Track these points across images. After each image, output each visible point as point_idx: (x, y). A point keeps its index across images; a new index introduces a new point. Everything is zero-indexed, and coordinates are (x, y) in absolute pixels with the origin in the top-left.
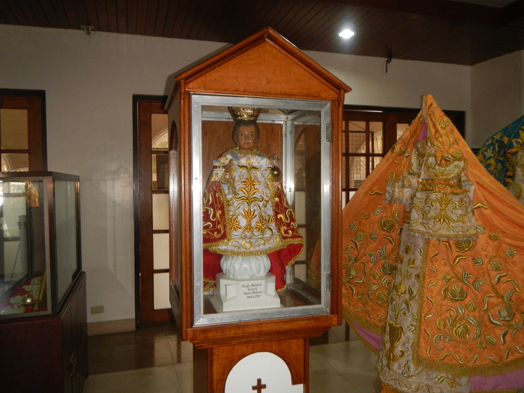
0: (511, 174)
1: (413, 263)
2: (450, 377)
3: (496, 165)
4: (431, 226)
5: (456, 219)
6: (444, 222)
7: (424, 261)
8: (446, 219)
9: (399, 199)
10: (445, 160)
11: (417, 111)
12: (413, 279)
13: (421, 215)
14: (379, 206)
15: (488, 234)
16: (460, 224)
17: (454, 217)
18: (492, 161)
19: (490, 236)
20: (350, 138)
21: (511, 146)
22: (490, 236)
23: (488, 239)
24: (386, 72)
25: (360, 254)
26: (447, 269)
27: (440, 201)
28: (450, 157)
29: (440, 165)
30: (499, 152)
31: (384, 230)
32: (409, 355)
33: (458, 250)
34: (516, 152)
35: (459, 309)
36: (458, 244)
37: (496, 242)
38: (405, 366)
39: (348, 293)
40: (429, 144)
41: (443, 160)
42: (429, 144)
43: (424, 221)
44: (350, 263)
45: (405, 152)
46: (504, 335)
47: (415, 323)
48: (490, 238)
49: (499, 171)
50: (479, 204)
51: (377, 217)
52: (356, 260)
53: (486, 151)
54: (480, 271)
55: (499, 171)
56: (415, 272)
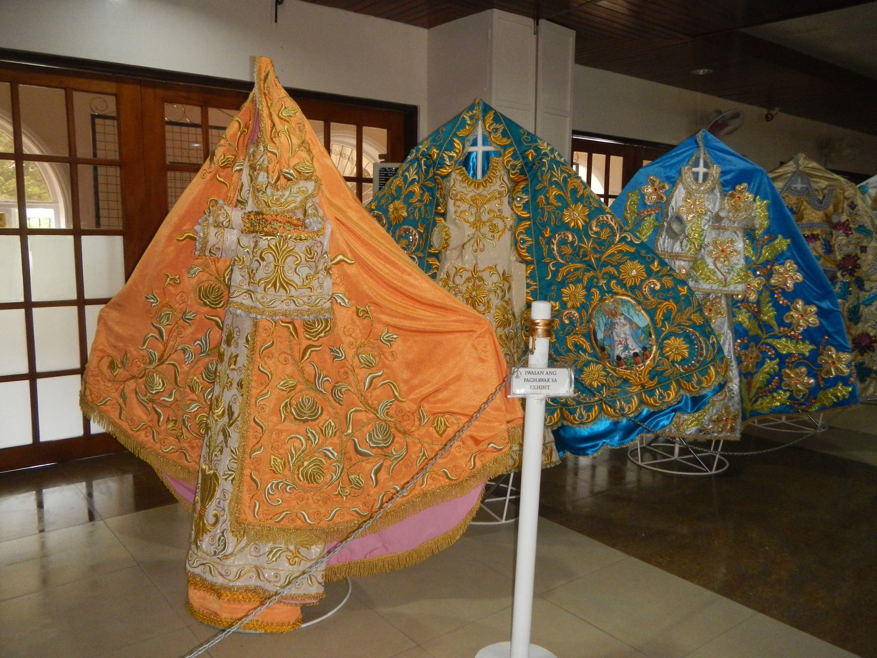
0: (443, 211)
1: (235, 362)
2: (292, 548)
3: (422, 195)
4: (259, 296)
5: (299, 284)
6: (281, 290)
7: (251, 359)
8: (285, 284)
9: (218, 249)
10: (285, 177)
11: (250, 86)
12: (234, 390)
13: (247, 277)
14: (196, 262)
15: (354, 308)
16: (307, 292)
17: (295, 278)
18: (416, 188)
19: (358, 310)
21: (442, 165)
22: (358, 310)
23: (355, 316)
24: (276, 21)
25: (168, 349)
26: (289, 369)
27: (277, 251)
28: (292, 172)
29: (275, 186)
30: (427, 172)
31: (205, 304)
32: (225, 524)
33: (308, 336)
34: (449, 174)
35: (310, 435)
36: (308, 326)
37: (366, 321)
38: (219, 539)
39: (151, 421)
40: (262, 148)
41: (282, 177)
42: (262, 148)
43: (251, 288)
44: (152, 367)
45: (234, 161)
46: (377, 472)
47: (235, 466)
48: (358, 315)
49: (426, 205)
50: (340, 257)
51: (194, 281)
52: (161, 361)
53: (408, 170)
54: (342, 370)
55: (426, 205)
56: (236, 377)
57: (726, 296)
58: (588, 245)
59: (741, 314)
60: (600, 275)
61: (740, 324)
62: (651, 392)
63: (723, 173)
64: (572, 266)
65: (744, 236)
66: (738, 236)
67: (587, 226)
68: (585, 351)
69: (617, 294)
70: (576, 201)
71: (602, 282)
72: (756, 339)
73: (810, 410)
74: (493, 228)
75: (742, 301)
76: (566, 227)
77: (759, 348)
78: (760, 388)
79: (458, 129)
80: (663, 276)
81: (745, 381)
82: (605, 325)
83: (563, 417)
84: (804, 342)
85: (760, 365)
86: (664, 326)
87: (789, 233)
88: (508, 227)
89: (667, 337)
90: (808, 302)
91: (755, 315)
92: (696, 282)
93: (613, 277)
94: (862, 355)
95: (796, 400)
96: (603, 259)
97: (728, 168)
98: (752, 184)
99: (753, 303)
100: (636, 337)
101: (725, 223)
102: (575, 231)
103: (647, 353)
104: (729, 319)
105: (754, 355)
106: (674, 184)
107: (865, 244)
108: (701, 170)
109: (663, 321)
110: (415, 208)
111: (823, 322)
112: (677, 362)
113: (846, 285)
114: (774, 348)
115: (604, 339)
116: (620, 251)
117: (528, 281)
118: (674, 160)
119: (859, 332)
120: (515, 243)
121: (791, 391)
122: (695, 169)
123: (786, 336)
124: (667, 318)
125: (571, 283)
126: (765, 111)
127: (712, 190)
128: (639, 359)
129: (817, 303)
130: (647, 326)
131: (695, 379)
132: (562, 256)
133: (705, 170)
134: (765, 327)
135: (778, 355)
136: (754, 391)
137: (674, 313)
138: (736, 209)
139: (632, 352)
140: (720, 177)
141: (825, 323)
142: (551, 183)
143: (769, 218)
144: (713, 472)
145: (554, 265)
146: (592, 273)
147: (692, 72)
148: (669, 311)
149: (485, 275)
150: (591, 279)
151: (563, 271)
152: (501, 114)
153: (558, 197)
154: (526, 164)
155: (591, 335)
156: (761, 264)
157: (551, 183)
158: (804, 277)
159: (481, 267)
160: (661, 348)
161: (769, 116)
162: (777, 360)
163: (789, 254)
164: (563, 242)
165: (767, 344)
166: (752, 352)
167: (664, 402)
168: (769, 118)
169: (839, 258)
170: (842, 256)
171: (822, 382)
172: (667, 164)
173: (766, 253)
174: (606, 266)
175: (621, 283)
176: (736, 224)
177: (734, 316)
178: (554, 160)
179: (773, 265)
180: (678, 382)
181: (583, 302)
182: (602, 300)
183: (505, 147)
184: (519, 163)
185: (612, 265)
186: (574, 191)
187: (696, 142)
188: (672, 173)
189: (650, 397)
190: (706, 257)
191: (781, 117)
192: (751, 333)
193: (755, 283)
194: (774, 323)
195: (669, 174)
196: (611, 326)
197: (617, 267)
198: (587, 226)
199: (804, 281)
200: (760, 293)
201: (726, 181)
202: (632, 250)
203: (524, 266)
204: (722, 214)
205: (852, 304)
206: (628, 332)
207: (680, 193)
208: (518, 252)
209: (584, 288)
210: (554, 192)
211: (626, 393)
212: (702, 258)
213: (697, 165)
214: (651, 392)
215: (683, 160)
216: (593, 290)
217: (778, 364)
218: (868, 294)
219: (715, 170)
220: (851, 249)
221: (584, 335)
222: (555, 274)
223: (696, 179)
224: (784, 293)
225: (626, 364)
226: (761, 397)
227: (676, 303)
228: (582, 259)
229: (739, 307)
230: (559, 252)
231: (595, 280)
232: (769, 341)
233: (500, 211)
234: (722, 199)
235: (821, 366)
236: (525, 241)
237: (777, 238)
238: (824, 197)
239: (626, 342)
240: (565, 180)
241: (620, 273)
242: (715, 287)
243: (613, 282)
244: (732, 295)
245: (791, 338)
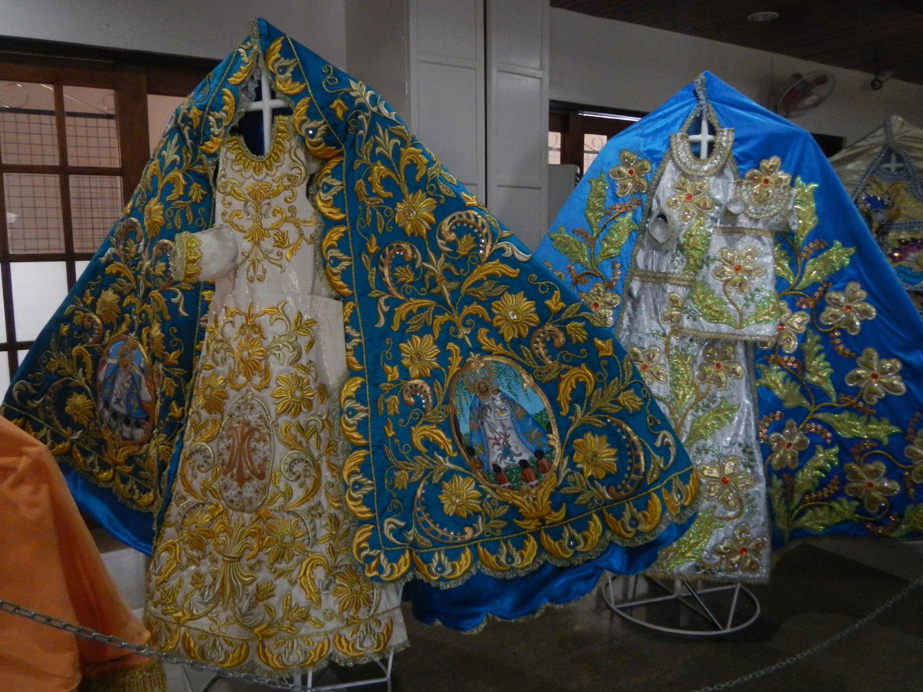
3: (187, 188)
20: (69, 130)
57: (745, 343)
58: (437, 266)
59: (771, 371)
60: (458, 319)
61: (768, 389)
62: (556, 534)
63: (738, 141)
64: (415, 304)
65: (775, 244)
66: (764, 244)
67: (434, 228)
68: (443, 453)
69: (489, 353)
70: (414, 188)
71: (464, 332)
72: (798, 414)
73: (894, 535)
74: (282, 241)
75: (773, 351)
76: (400, 233)
77: (803, 429)
78: (808, 493)
79: (229, 75)
80: (569, 320)
81: (778, 483)
82: (471, 409)
83: (413, 566)
84: (879, 420)
85: (805, 455)
86: (572, 412)
87: (852, 238)
88: (308, 236)
89: (578, 434)
90: (886, 354)
91: (796, 375)
92: (695, 320)
93: (480, 322)
95: (867, 514)
96: (463, 289)
97: (745, 132)
98: (789, 156)
99: (790, 355)
100: (524, 435)
101: (743, 222)
102: (416, 240)
103: (544, 461)
104: (748, 381)
106: (657, 159)
108: (704, 137)
109: (571, 404)
110: (175, 210)
111: (912, 387)
112: (598, 480)
114: (831, 429)
115: (471, 435)
116: (492, 277)
117: (349, 329)
118: (660, 124)
120: (324, 264)
121: (861, 501)
123: (851, 409)
124: (579, 395)
125: (416, 333)
126: (870, 77)
127: (720, 172)
128: (530, 472)
129: (901, 355)
130: (545, 410)
131: (627, 516)
132: (399, 286)
133: (711, 137)
134: (813, 393)
135: (837, 440)
136: (797, 497)
137: (590, 388)
138: (762, 200)
139: (517, 459)
140: (733, 147)
141: (912, 387)
142: (374, 157)
143: (817, 212)
144: (729, 630)
145: (387, 302)
146: (447, 317)
147: (749, 17)
148: (581, 386)
149: (264, 320)
150: (447, 325)
151: (401, 311)
152: (292, 40)
153: (387, 183)
154: (335, 126)
155: (451, 426)
156: (803, 290)
157: (374, 157)
158: (878, 311)
159: (257, 309)
160: (569, 451)
161: (876, 83)
162: (835, 450)
163: (851, 272)
164: (400, 261)
165: (818, 421)
166: (791, 436)
167: (577, 553)
168: (876, 85)
171: (912, 490)
172: (649, 130)
173: (813, 272)
174: (469, 303)
175: (496, 334)
176: (760, 225)
177: (758, 376)
178: (377, 117)
179: (825, 291)
180: (601, 515)
181: (435, 369)
182: (463, 364)
183: (296, 97)
184: (321, 126)
185: (480, 302)
186: (412, 168)
187: (696, 94)
188: (657, 145)
189: (555, 540)
190: (711, 280)
191: (893, 85)
192: (789, 404)
193: (798, 320)
194: (829, 387)
195: (651, 147)
196: (479, 412)
197: (487, 304)
198: (434, 228)
199: (877, 317)
200: (802, 338)
201: (743, 154)
202: (513, 272)
203: (340, 304)
204: (734, 209)
206: (508, 424)
207: (668, 179)
208: (329, 279)
209: (435, 342)
210: (379, 169)
211: (518, 529)
212: (705, 283)
213: (698, 131)
214: (556, 534)
215: (673, 123)
216: (451, 346)
217: (837, 455)
219: (726, 137)
221: (439, 426)
222: (389, 316)
223: (697, 155)
225: (510, 480)
226: (811, 507)
227: (594, 371)
228: (429, 290)
229: (766, 363)
230: (394, 279)
231: (452, 329)
232: (820, 416)
233: (292, 210)
234: (739, 184)
235: (909, 462)
236: (337, 261)
237: (832, 245)
239: (506, 441)
240: (396, 150)
241: (492, 315)
242: (724, 328)
243: (483, 331)
244: (755, 343)
245: (859, 412)
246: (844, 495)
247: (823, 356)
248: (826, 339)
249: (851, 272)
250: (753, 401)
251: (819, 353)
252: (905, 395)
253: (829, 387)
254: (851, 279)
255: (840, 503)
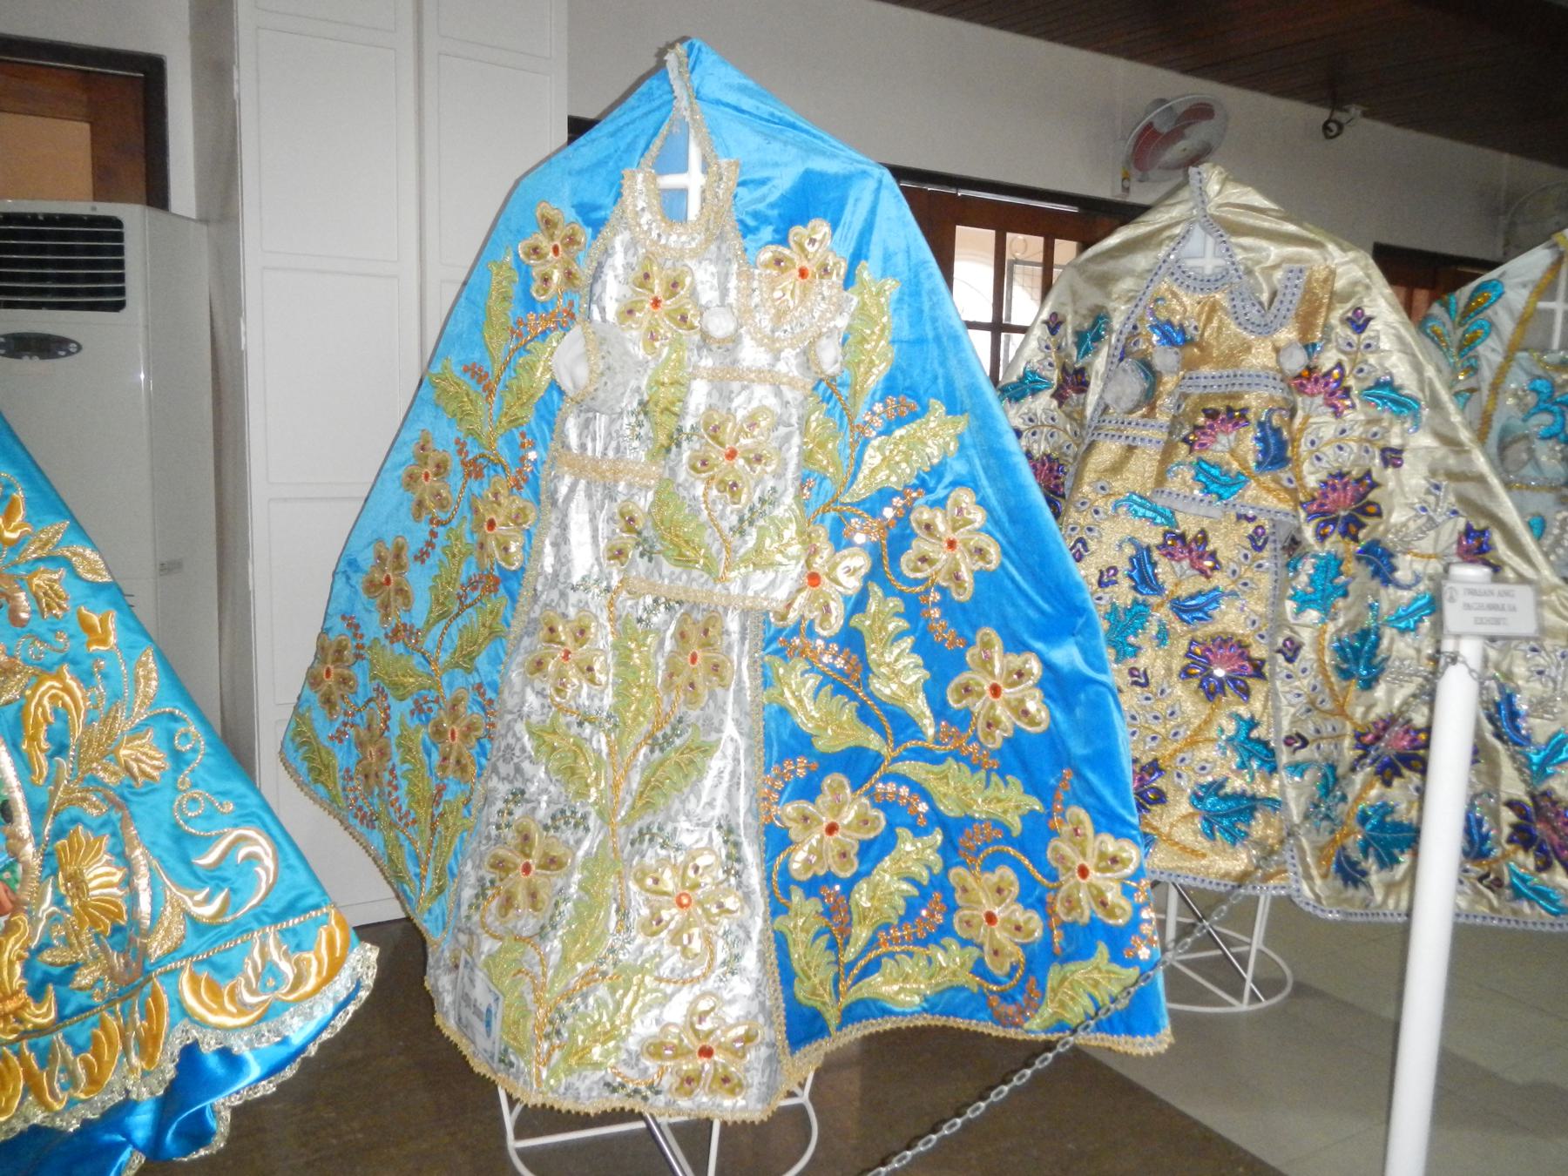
72: (856, 765)
85: (872, 851)
90: (1015, 645)
94: (1388, 784)
99: (828, 641)
105: (849, 815)
107: (1395, 442)
113: (1331, 567)
114: (926, 796)
119: (1379, 711)
122: (670, 181)
123: (957, 756)
126: (1320, 114)
129: (1039, 645)
136: (861, 934)
141: (1059, 715)
161: (1333, 126)
165: (902, 779)
166: (838, 807)
168: (1329, 130)
169: (1312, 481)
170: (1323, 476)
192: (827, 743)
194: (919, 706)
205: (1350, 624)
218: (1406, 595)
220: (1349, 459)
224: (947, 604)
232: (904, 767)
237: (925, 409)
238: (1274, 294)
246: (954, 934)
247: (908, 642)
248: (914, 610)
249: (959, 467)
250: (749, 736)
251: (900, 636)
252: (1048, 732)
253: (919, 706)
254: (955, 484)
255: (944, 948)
